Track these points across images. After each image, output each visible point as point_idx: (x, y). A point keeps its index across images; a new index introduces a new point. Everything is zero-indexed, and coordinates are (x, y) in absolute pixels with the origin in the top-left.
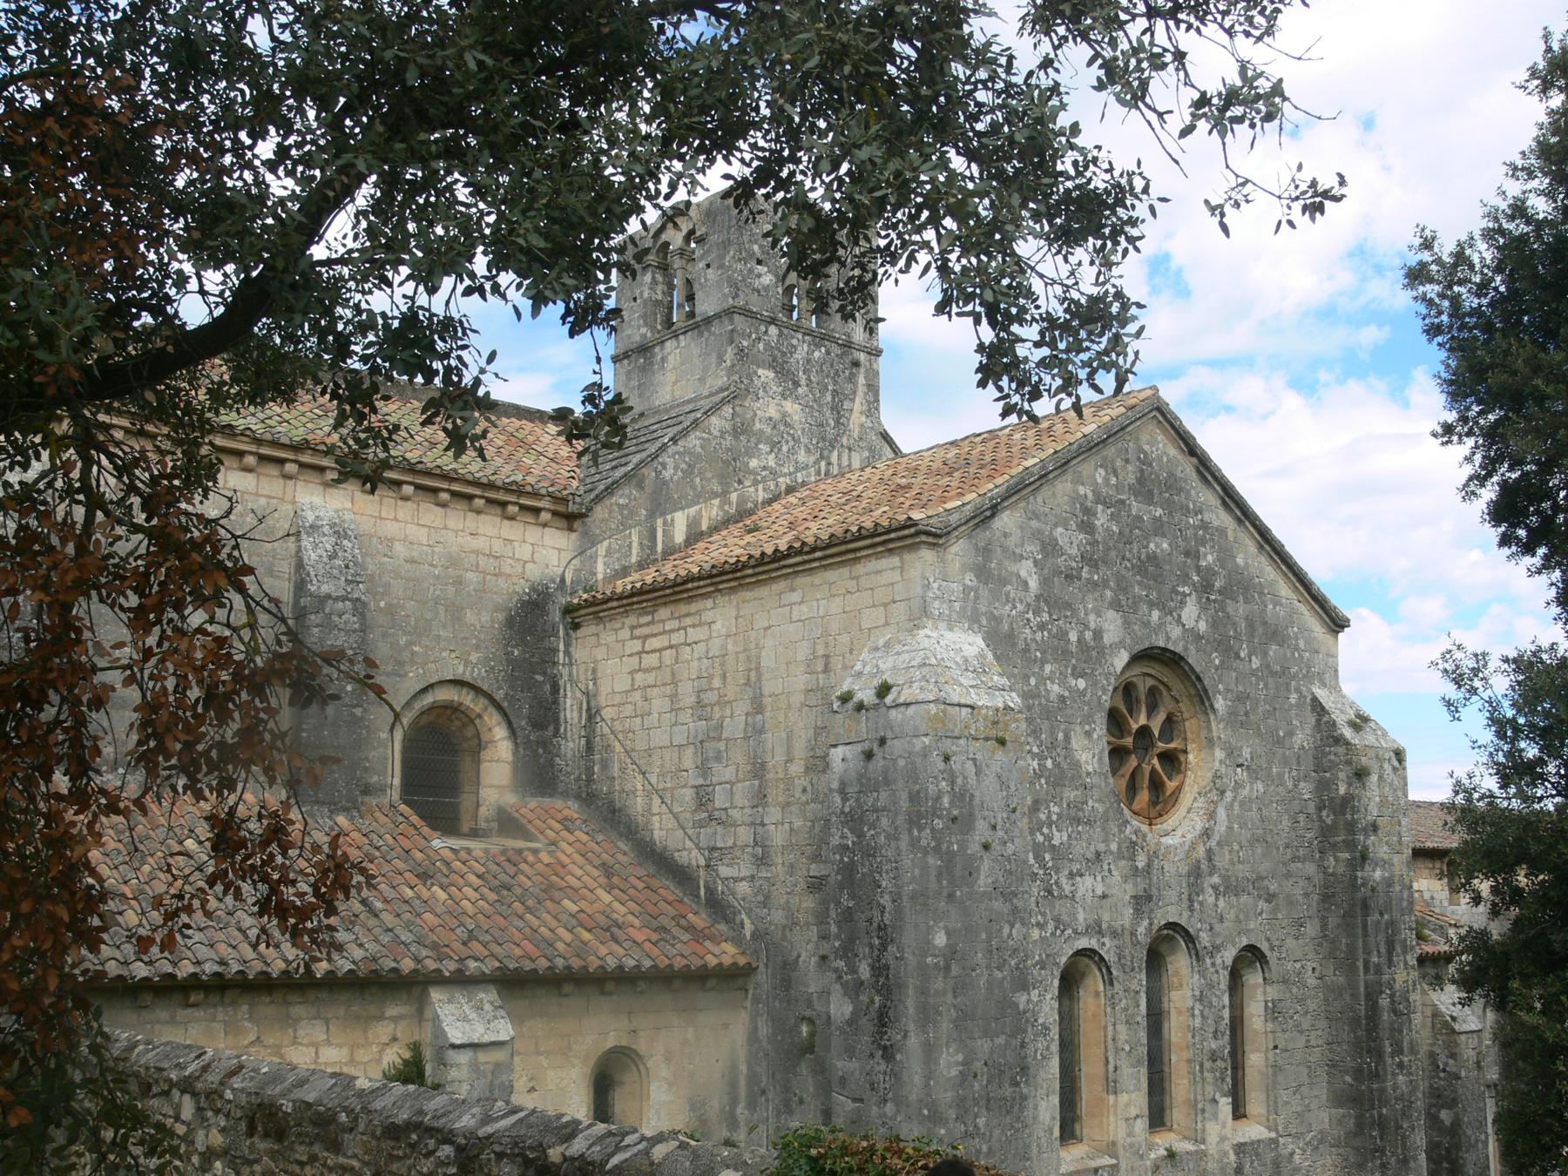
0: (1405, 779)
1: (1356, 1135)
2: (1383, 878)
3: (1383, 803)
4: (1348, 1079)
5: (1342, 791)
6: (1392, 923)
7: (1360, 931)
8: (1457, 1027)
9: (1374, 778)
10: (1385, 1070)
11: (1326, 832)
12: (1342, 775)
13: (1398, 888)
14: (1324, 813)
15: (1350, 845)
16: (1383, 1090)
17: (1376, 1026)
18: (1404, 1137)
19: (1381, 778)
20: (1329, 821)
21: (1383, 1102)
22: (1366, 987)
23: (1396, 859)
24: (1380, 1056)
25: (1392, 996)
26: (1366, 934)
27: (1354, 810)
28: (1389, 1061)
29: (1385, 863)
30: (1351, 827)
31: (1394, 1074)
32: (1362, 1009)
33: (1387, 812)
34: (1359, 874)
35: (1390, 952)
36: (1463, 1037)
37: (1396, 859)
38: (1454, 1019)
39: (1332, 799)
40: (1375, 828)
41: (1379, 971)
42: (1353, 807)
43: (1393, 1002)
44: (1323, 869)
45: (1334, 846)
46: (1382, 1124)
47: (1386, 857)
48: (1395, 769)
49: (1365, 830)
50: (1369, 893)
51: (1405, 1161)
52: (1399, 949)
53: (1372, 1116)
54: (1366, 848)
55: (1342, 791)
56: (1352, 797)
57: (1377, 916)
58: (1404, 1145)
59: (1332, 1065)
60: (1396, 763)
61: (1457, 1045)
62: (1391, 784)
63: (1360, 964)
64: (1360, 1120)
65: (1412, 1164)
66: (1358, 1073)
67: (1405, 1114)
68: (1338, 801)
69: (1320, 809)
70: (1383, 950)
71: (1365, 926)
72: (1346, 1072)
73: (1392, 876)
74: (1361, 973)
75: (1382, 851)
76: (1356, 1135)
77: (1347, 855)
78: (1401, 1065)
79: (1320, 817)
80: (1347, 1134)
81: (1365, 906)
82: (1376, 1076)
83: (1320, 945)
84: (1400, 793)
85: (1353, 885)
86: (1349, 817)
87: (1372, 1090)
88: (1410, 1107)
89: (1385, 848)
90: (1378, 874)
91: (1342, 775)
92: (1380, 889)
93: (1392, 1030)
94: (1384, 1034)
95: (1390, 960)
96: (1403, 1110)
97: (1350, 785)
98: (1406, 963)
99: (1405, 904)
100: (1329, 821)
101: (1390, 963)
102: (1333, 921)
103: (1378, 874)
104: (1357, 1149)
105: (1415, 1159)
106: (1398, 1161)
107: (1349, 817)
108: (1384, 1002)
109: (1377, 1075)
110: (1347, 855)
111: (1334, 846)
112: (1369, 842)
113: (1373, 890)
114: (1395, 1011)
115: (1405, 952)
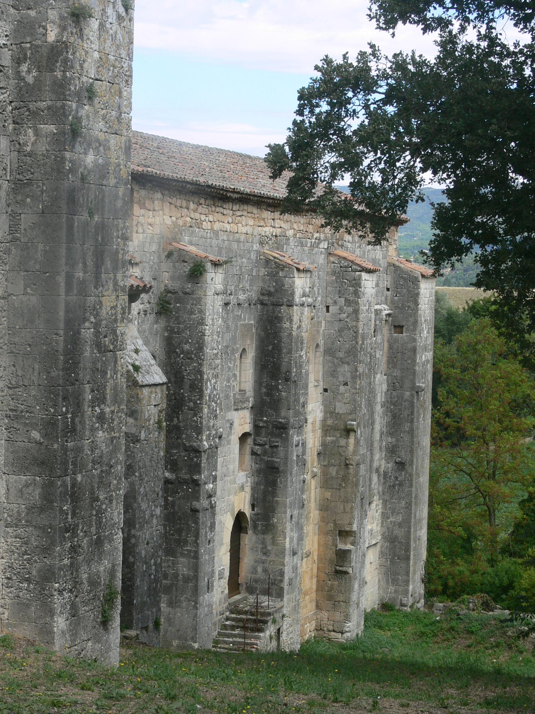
0: (130, 33)
1: (42, 510)
2: (96, 165)
3: (102, 63)
4: (36, 435)
5: (52, 37)
6: (102, 227)
7: (63, 234)
8: (140, 379)
9: (94, 24)
10: (83, 423)
11: (25, 94)
12: (53, 15)
13: (113, 181)
14: (24, 68)
15: (58, 114)
16: (79, 450)
17: (76, 364)
18: (100, 512)
19: (102, 26)
20: (30, 79)
21: (78, 466)
22: (67, 311)
23: (113, 141)
24: (79, 405)
25: (97, 325)
26: (70, 240)
27: (67, 65)
28: (88, 411)
29: (101, 146)
30: (61, 88)
31: (93, 430)
32: (60, 342)
33: (107, 75)
34: (68, 155)
35: (98, 266)
36: (146, 391)
37: (113, 141)
38: (137, 368)
39: (35, 48)
40: (90, 94)
41: (83, 292)
42: (66, 61)
43: (97, 333)
44: (17, 146)
45: (35, 114)
46: (74, 495)
47: (102, 136)
48: (119, 18)
49: (78, 94)
50: (78, 183)
51: (99, 543)
52: (108, 264)
53: (64, 484)
54: (78, 119)
55: (52, 37)
56: (66, 46)
57: (84, 216)
58: (99, 523)
59: (15, 416)
60: (122, 10)
61: (139, 400)
62: (114, 38)
63: (61, 280)
64: (48, 489)
65: (107, 547)
66: (49, 427)
67: (103, 483)
68: (44, 51)
69: (18, 61)
70: (90, 263)
71: (70, 227)
72: (34, 426)
73: (107, 164)
74: (62, 290)
75: (97, 128)
76: (42, 510)
77: (52, 128)
78: (101, 418)
79: (19, 77)
80: (30, 509)
81: (72, 201)
82: (72, 431)
83: (7, 252)
84: (124, 54)
85: (58, 169)
86: (59, 74)
87: (65, 450)
88: (108, 473)
89: (101, 125)
90: (90, 159)
91: (53, 15)
92: (92, 178)
93: (94, 370)
94: (85, 375)
95: (97, 277)
96: (101, 477)
97: (63, 28)
98: (116, 284)
99: (119, 203)
100: (30, 79)
101: (98, 282)
102: (27, 220)
103: (90, 159)
104: (43, 529)
105: (111, 540)
106: (90, 544)
107: (59, 74)
108: (87, 333)
109: (74, 430)
110: (52, 128)
111: (35, 114)
112: (82, 113)
113: (83, 179)
114: (99, 346)
115: (115, 269)
